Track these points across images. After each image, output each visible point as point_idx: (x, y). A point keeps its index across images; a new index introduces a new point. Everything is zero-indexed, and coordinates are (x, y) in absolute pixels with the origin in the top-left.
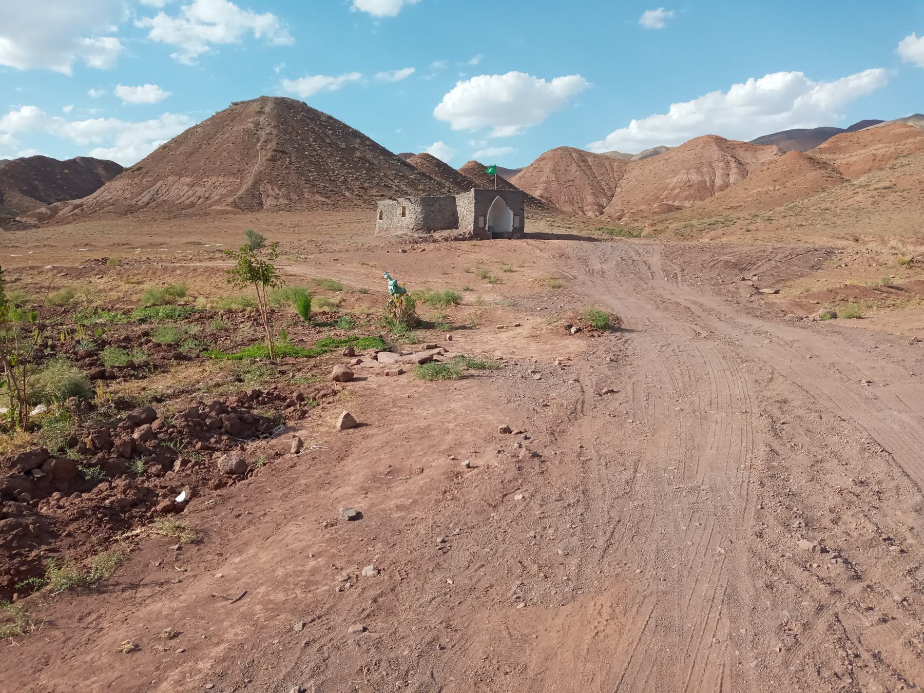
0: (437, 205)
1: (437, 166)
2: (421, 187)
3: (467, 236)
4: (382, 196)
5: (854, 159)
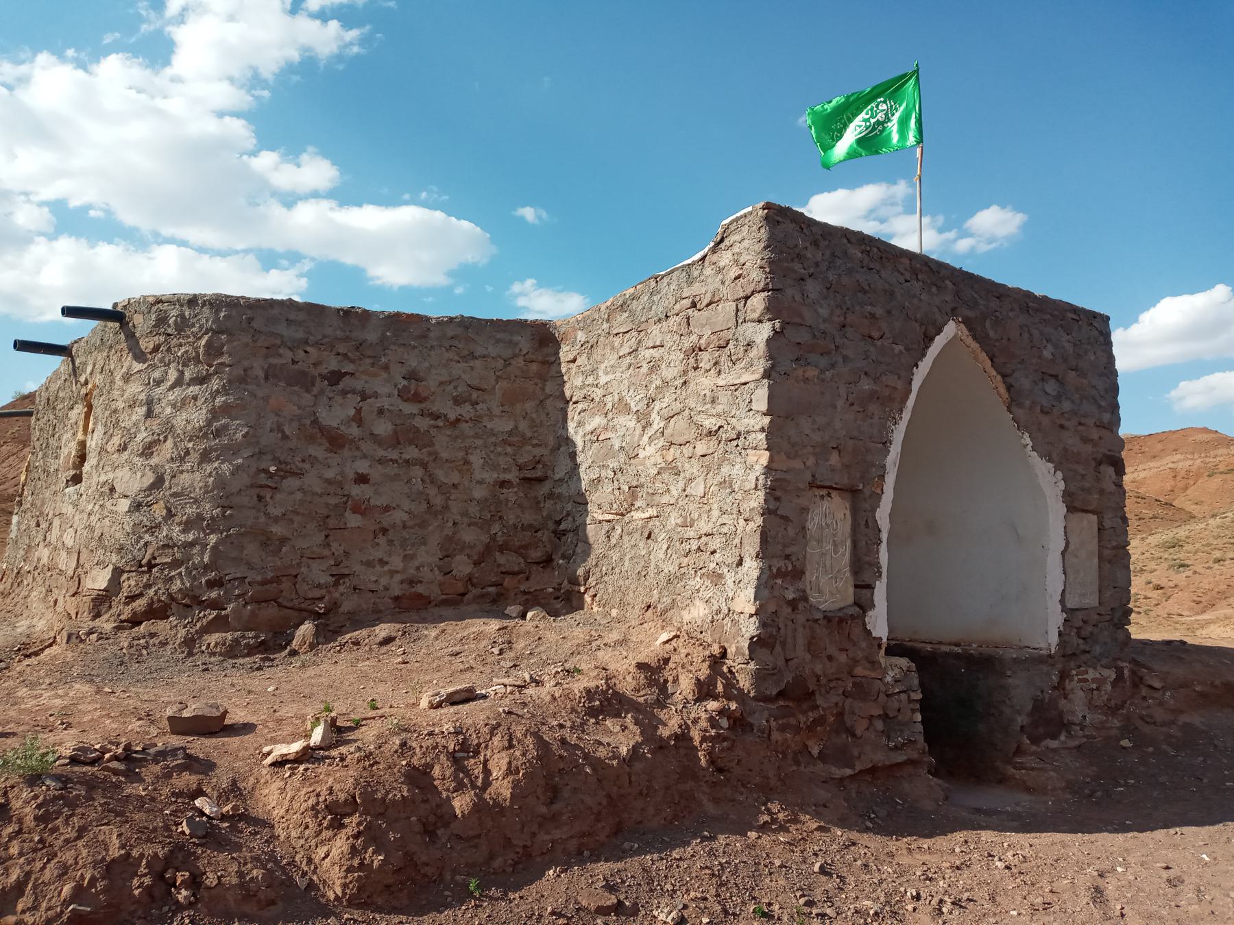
0: (384, 388)
3: (688, 715)
5: (1142, 475)
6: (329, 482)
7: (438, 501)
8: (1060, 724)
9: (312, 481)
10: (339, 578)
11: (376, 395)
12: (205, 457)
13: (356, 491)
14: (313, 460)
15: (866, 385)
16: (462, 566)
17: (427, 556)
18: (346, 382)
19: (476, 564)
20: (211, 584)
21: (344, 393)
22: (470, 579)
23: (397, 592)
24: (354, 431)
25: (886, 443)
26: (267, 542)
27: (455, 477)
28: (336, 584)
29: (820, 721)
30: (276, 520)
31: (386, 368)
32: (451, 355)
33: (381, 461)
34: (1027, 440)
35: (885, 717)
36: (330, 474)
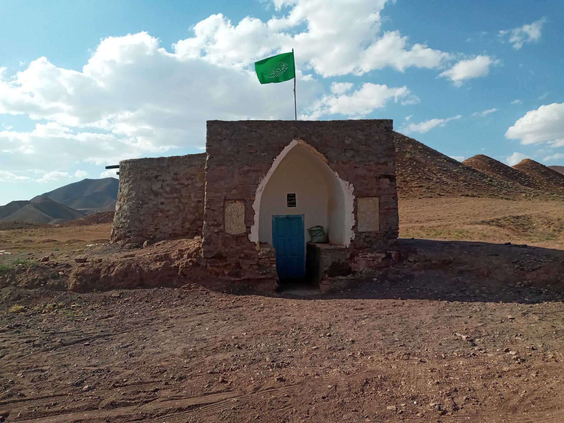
0: (168, 178)
1: (489, 164)
2: (461, 178)
4: (420, 187)
6: (154, 205)
7: (182, 207)
8: (348, 271)
9: (150, 205)
10: (156, 229)
11: (166, 180)
12: (128, 201)
13: (161, 207)
14: (151, 199)
15: (246, 168)
16: (187, 225)
17: (178, 223)
18: (159, 178)
19: (191, 224)
20: (128, 232)
21: (158, 181)
22: (189, 229)
23: (170, 233)
24: (161, 191)
25: (257, 185)
26: (141, 221)
27: (186, 201)
28: (156, 231)
29: (229, 265)
30: (142, 215)
31: (169, 172)
32: (186, 166)
33: (167, 198)
34: (337, 174)
35: (258, 264)
36: (155, 203)
